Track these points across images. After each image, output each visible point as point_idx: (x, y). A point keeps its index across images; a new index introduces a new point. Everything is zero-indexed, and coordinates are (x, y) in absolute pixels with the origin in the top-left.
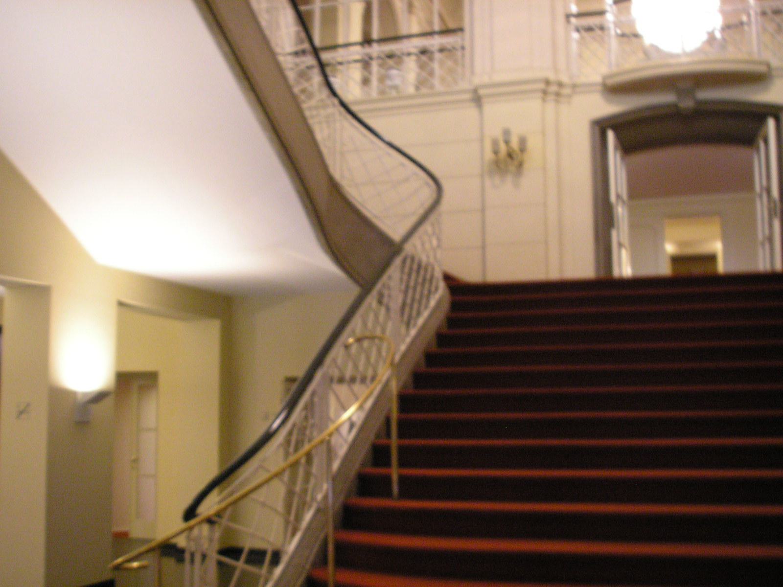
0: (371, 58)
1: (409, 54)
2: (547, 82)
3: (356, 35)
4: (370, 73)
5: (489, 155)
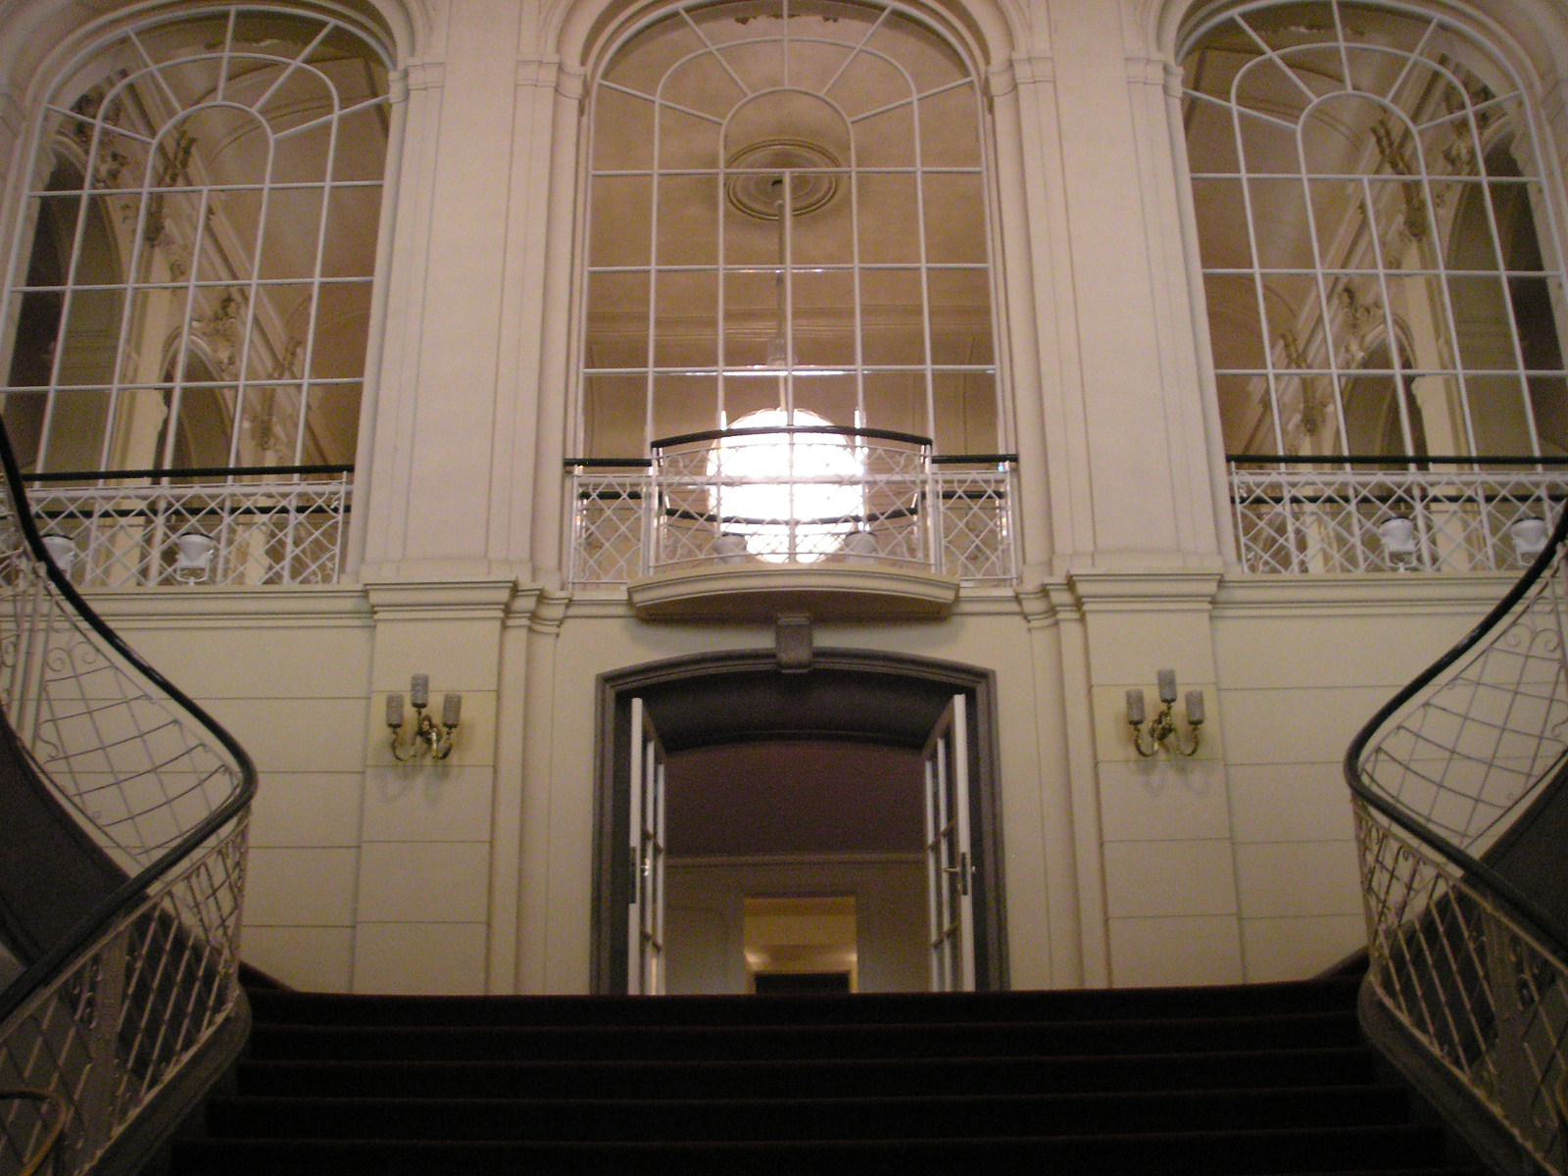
2: (515, 590)
5: (380, 732)
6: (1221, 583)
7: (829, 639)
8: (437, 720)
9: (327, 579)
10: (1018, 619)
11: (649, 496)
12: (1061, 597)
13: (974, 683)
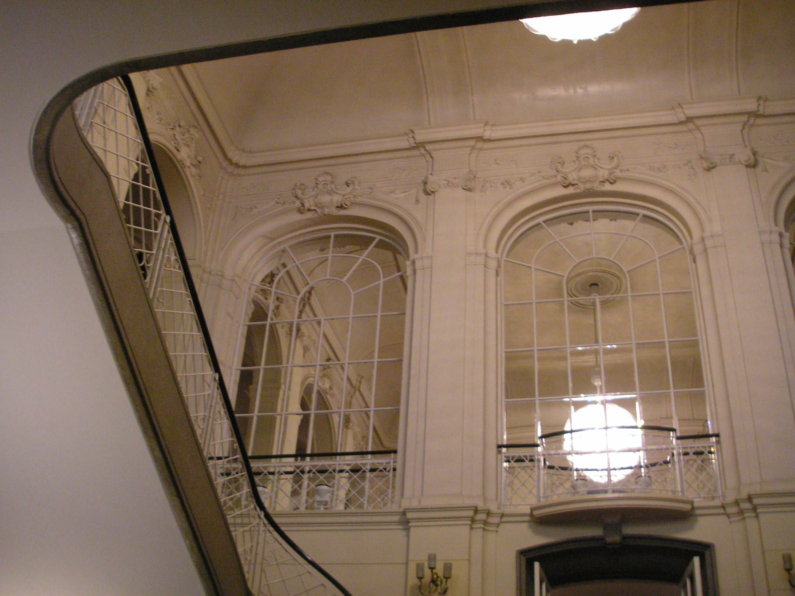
0: (303, 472)
1: (341, 471)
2: (476, 511)
3: (291, 449)
4: (300, 486)
5: (413, 580)
7: (629, 530)
8: (441, 574)
9: (385, 505)
10: (725, 517)
11: (539, 461)
12: (747, 506)
13: (703, 550)
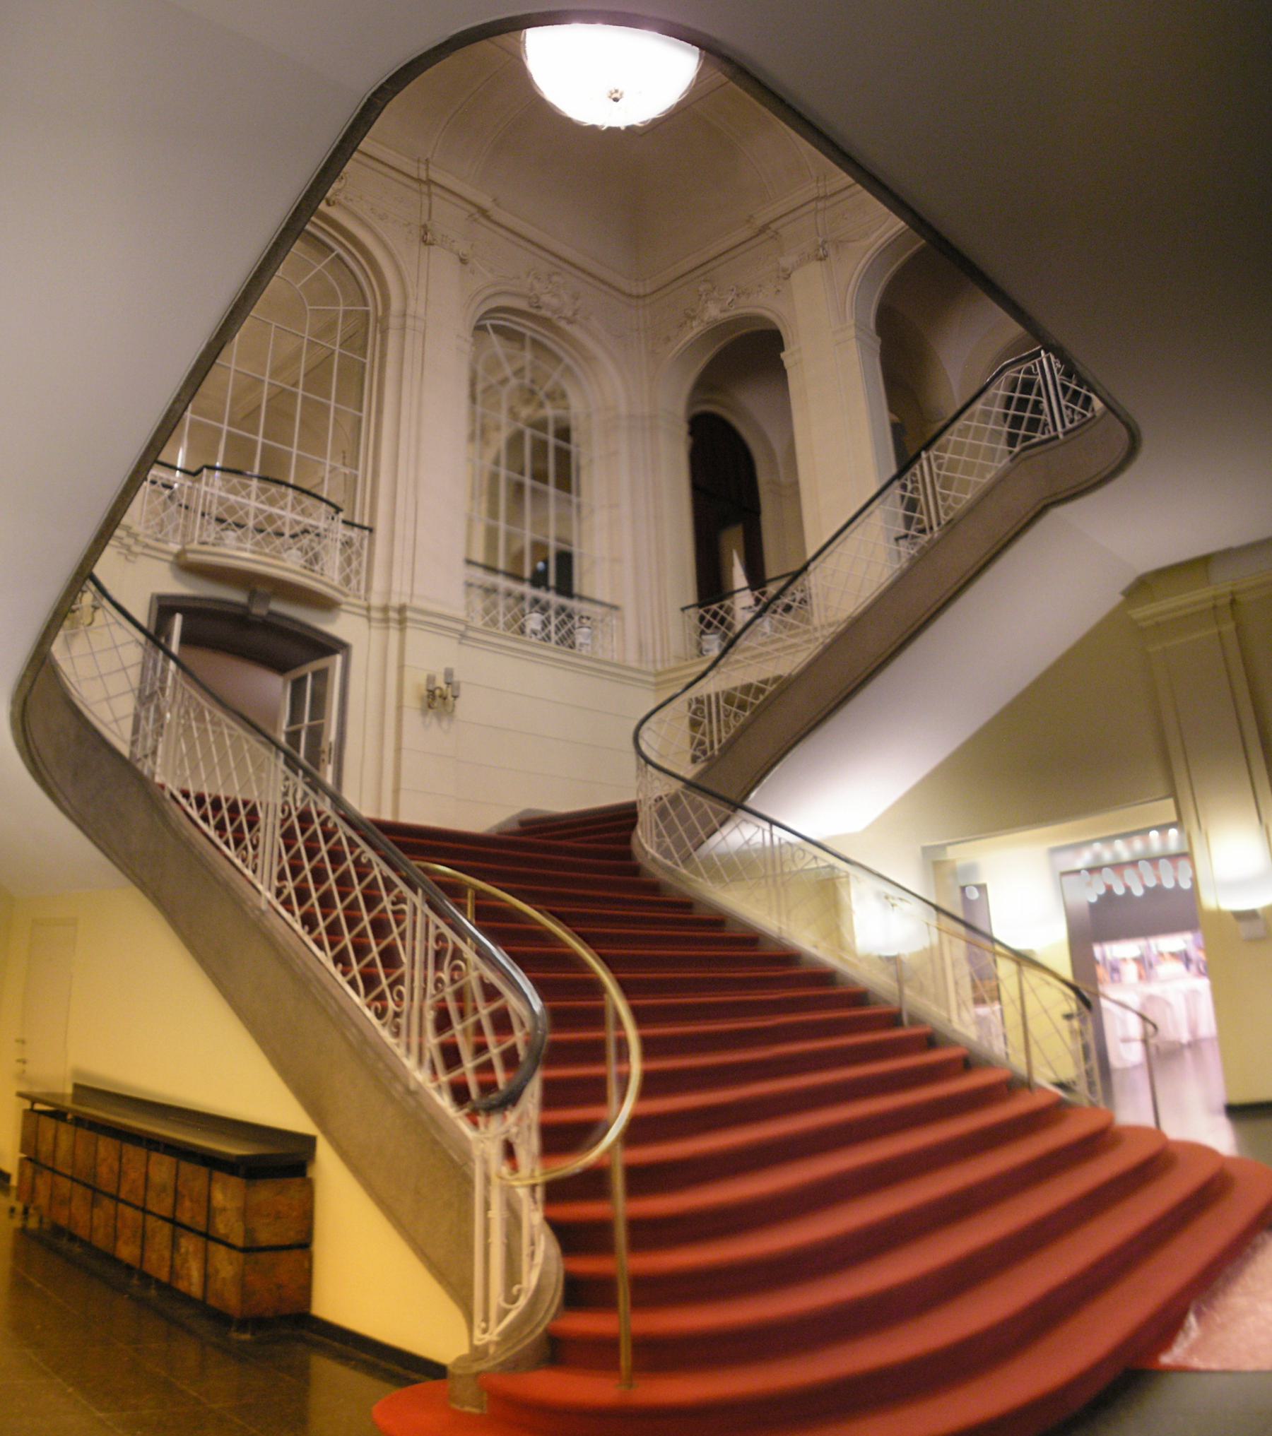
6: (468, 627)
7: (278, 607)
12: (393, 615)
